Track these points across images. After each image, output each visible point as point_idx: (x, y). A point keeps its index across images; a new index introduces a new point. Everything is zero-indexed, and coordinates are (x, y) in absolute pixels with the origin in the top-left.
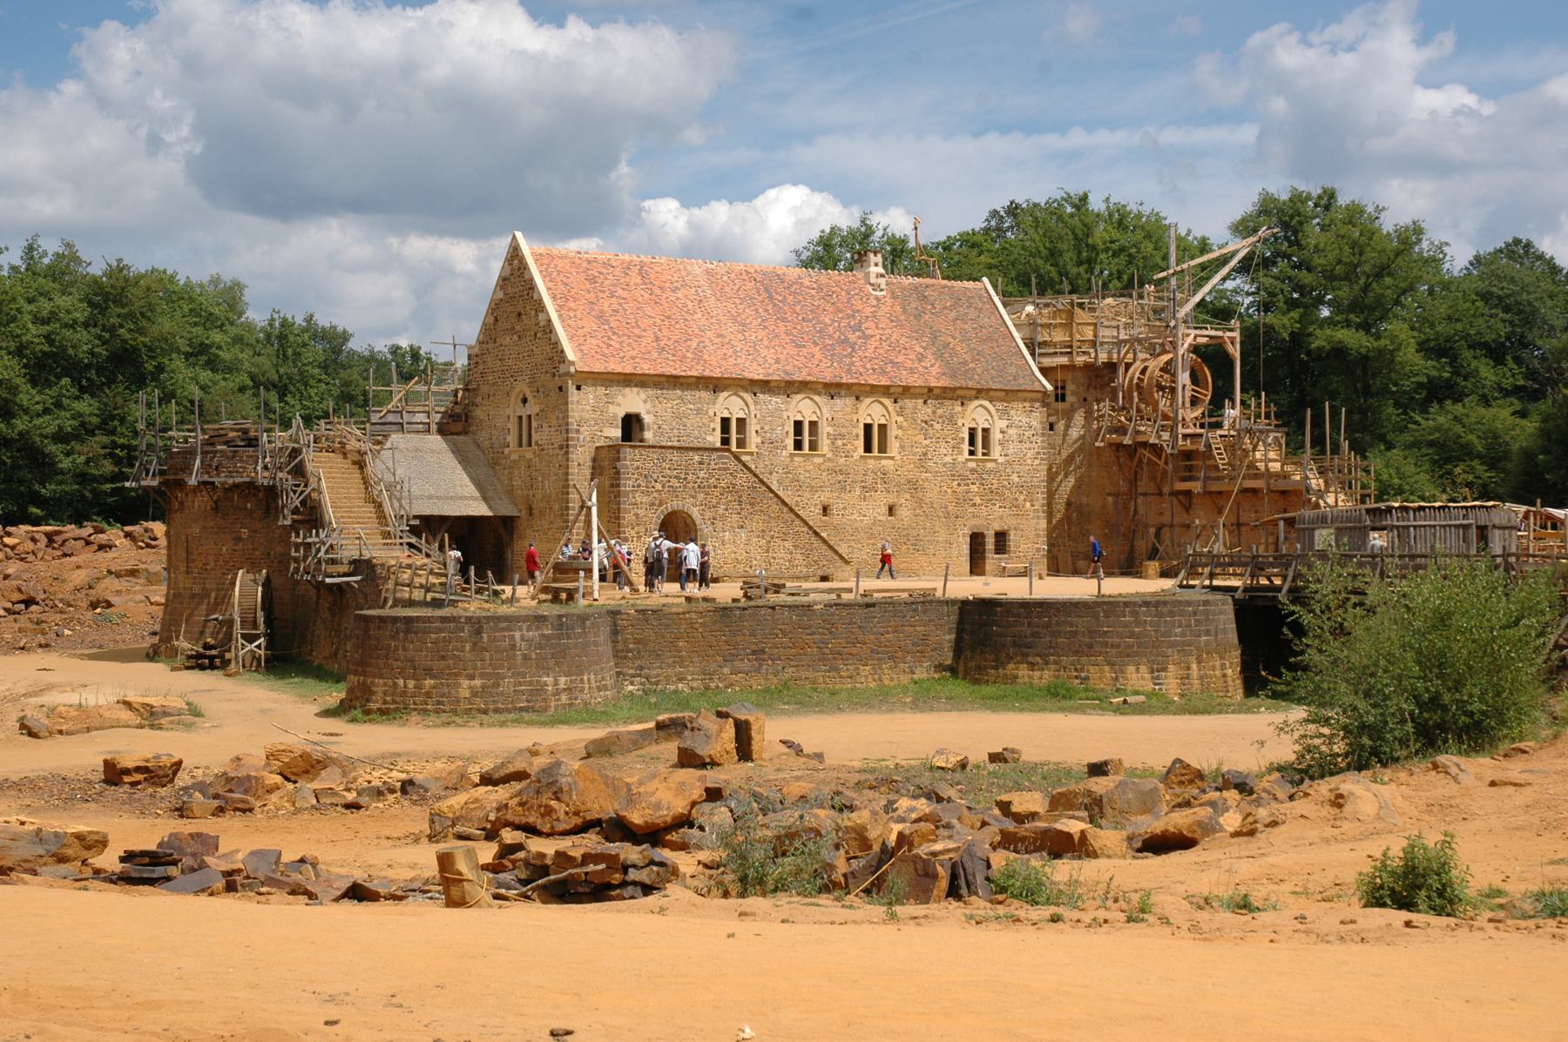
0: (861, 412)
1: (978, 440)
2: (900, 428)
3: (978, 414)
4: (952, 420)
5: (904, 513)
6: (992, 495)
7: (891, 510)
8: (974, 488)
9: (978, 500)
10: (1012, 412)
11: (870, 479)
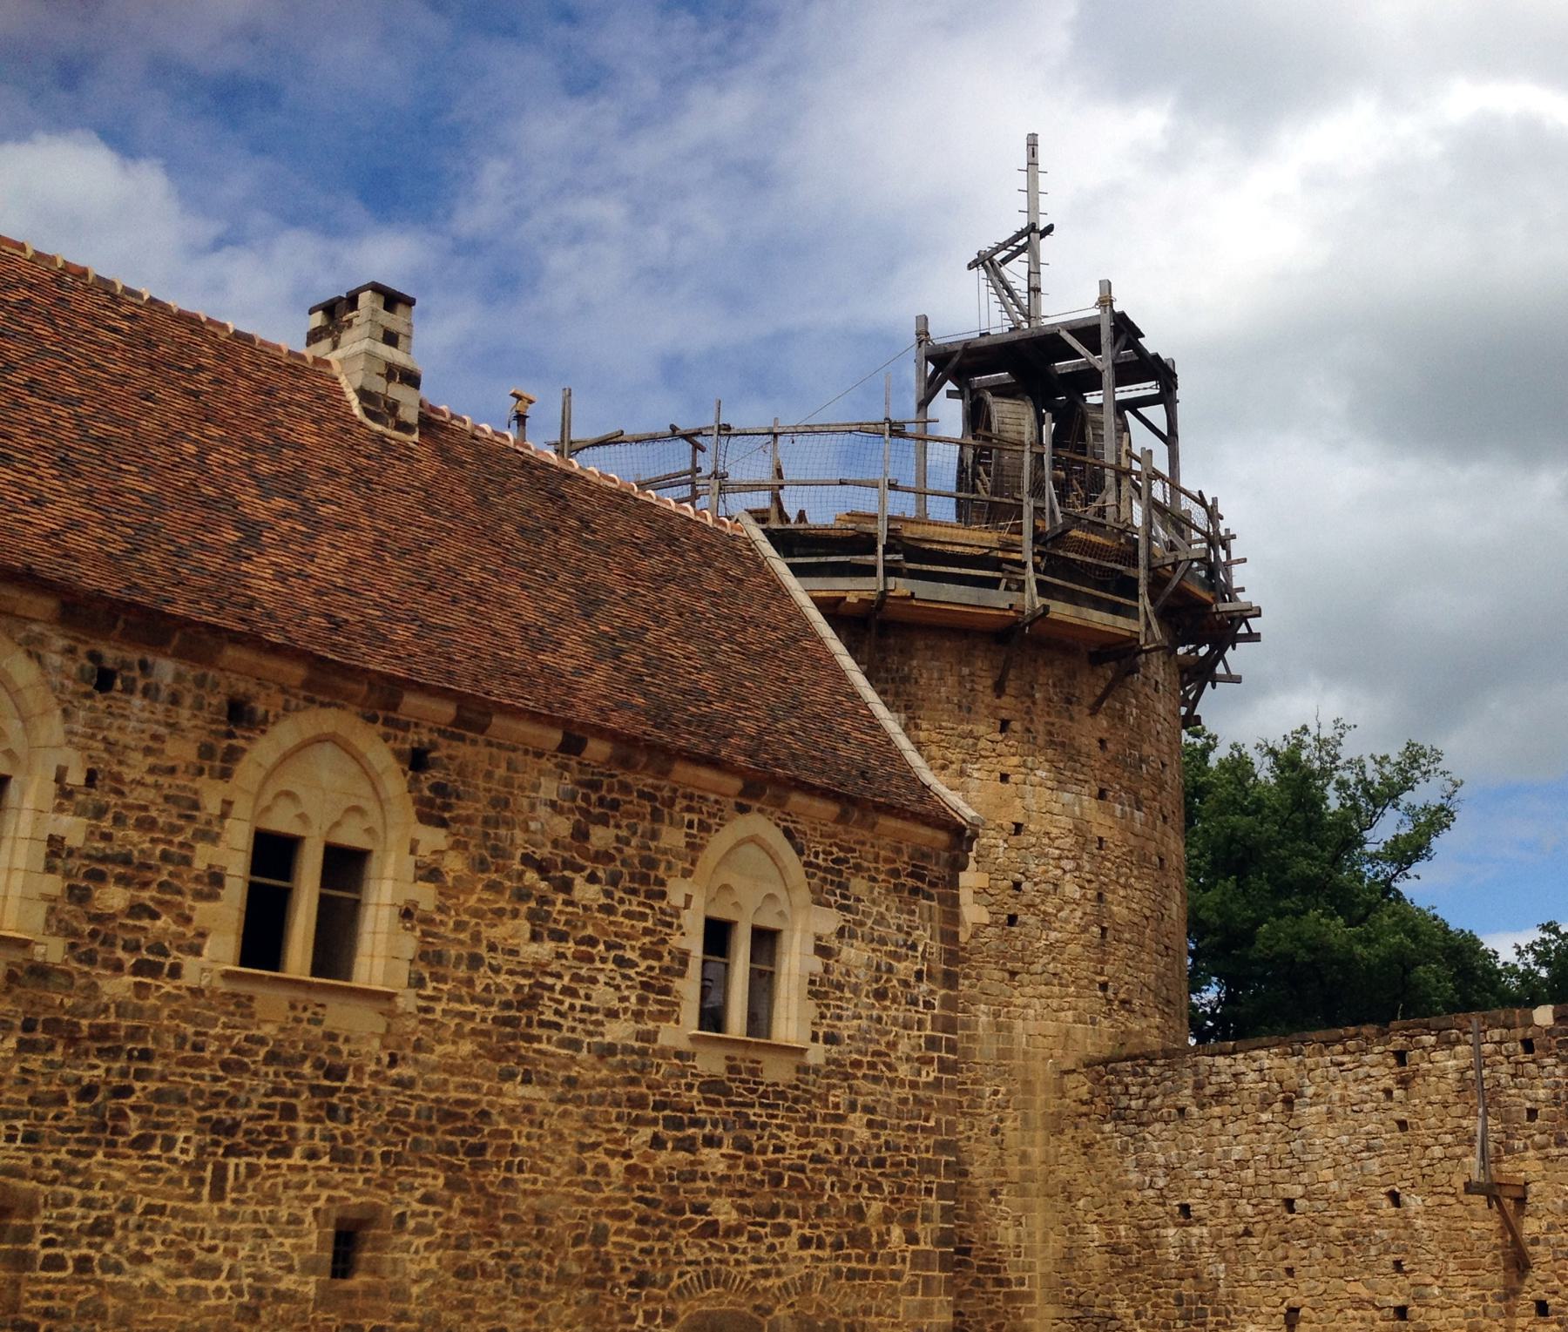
0: (248, 772)
2: (431, 874)
5: (412, 1261)
6: (775, 1195)
7: (347, 1243)
9: (724, 1212)
11: (258, 1085)
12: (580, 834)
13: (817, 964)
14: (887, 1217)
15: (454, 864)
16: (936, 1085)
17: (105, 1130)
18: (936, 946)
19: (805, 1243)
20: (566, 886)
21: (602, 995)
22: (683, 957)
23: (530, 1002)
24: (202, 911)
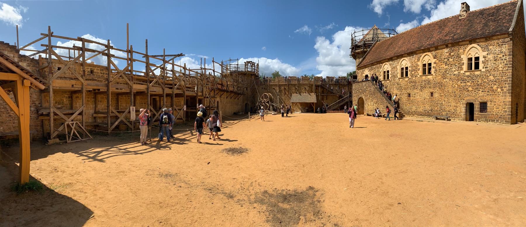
0: (421, 60)
1: (474, 64)
2: (435, 63)
3: (475, 50)
4: (459, 56)
5: (436, 95)
6: (478, 87)
7: (432, 93)
8: (469, 84)
9: (470, 89)
10: (490, 47)
11: (423, 83)
12: (450, 54)
13: (483, 59)
14: (497, 88)
15: (437, 61)
16: (507, 70)
17: (414, 88)
18: (507, 51)
19: (482, 91)
20: (448, 60)
21: (454, 69)
22: (463, 63)
23: (446, 72)
24: (419, 72)
